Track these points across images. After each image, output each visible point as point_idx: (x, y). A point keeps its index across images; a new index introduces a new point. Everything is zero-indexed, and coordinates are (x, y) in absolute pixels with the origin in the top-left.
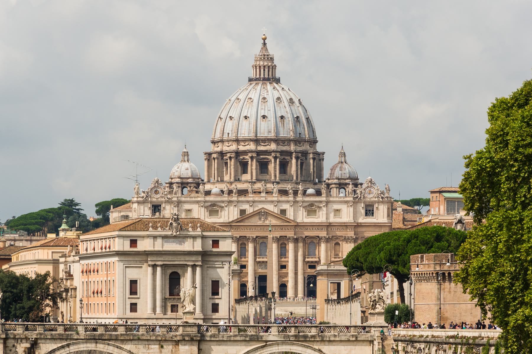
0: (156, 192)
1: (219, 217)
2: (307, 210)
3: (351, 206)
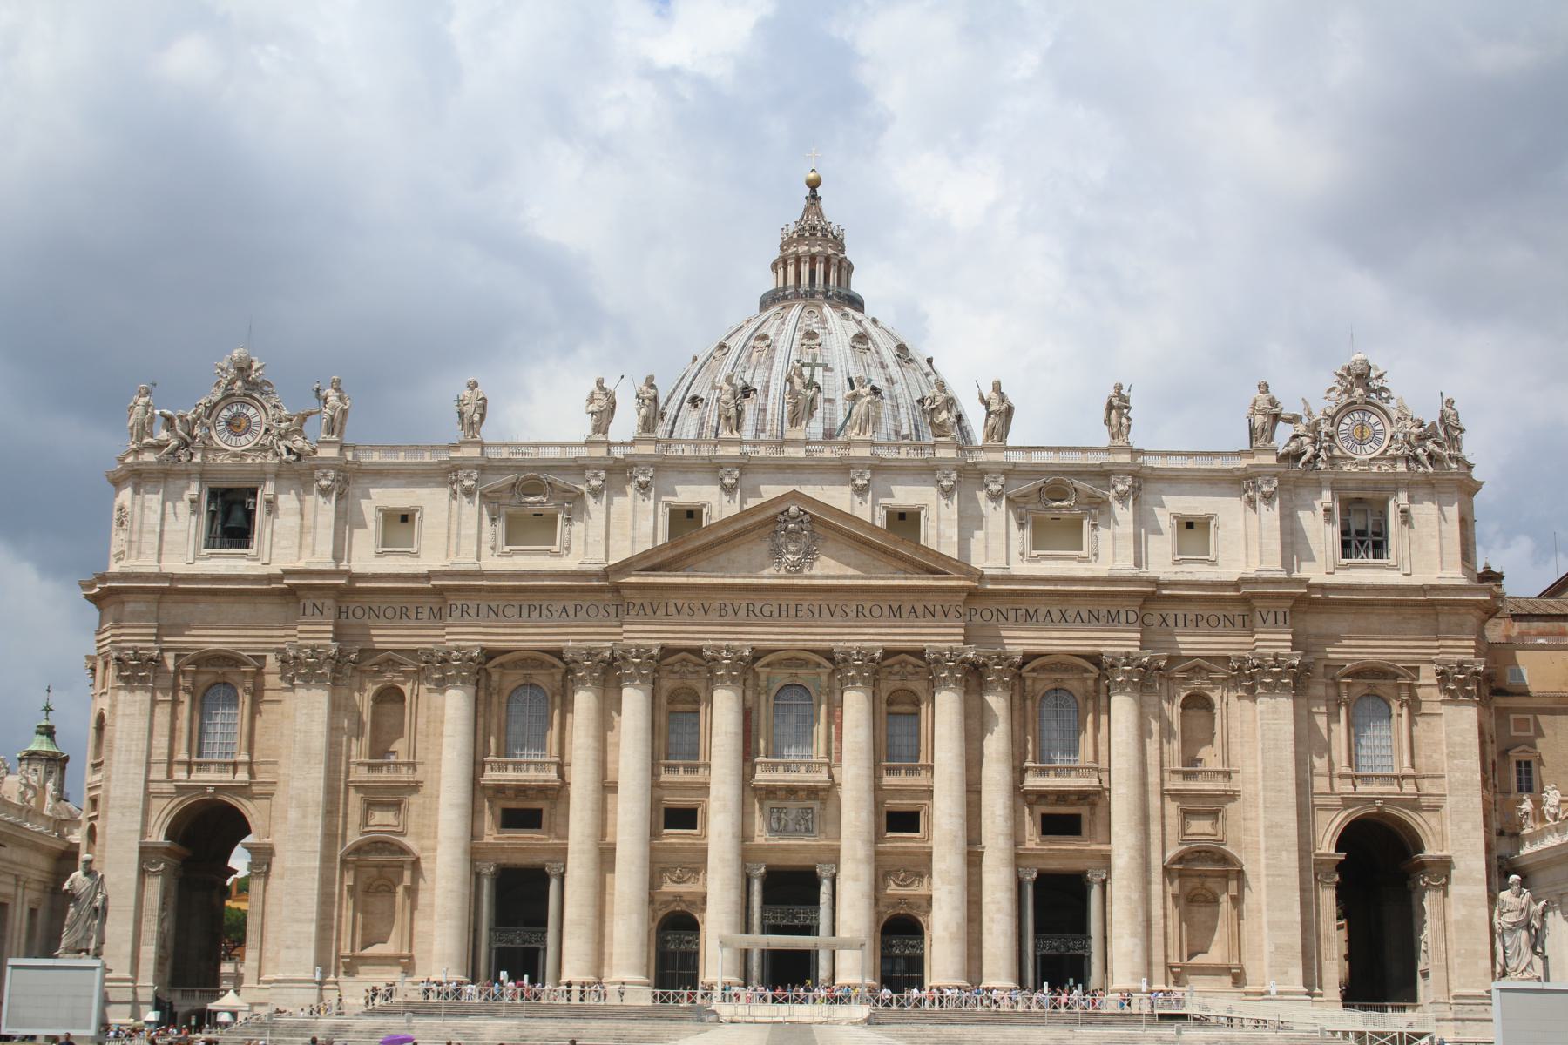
0: (236, 426)
1: (556, 548)
2: (1030, 517)
3: (1268, 498)
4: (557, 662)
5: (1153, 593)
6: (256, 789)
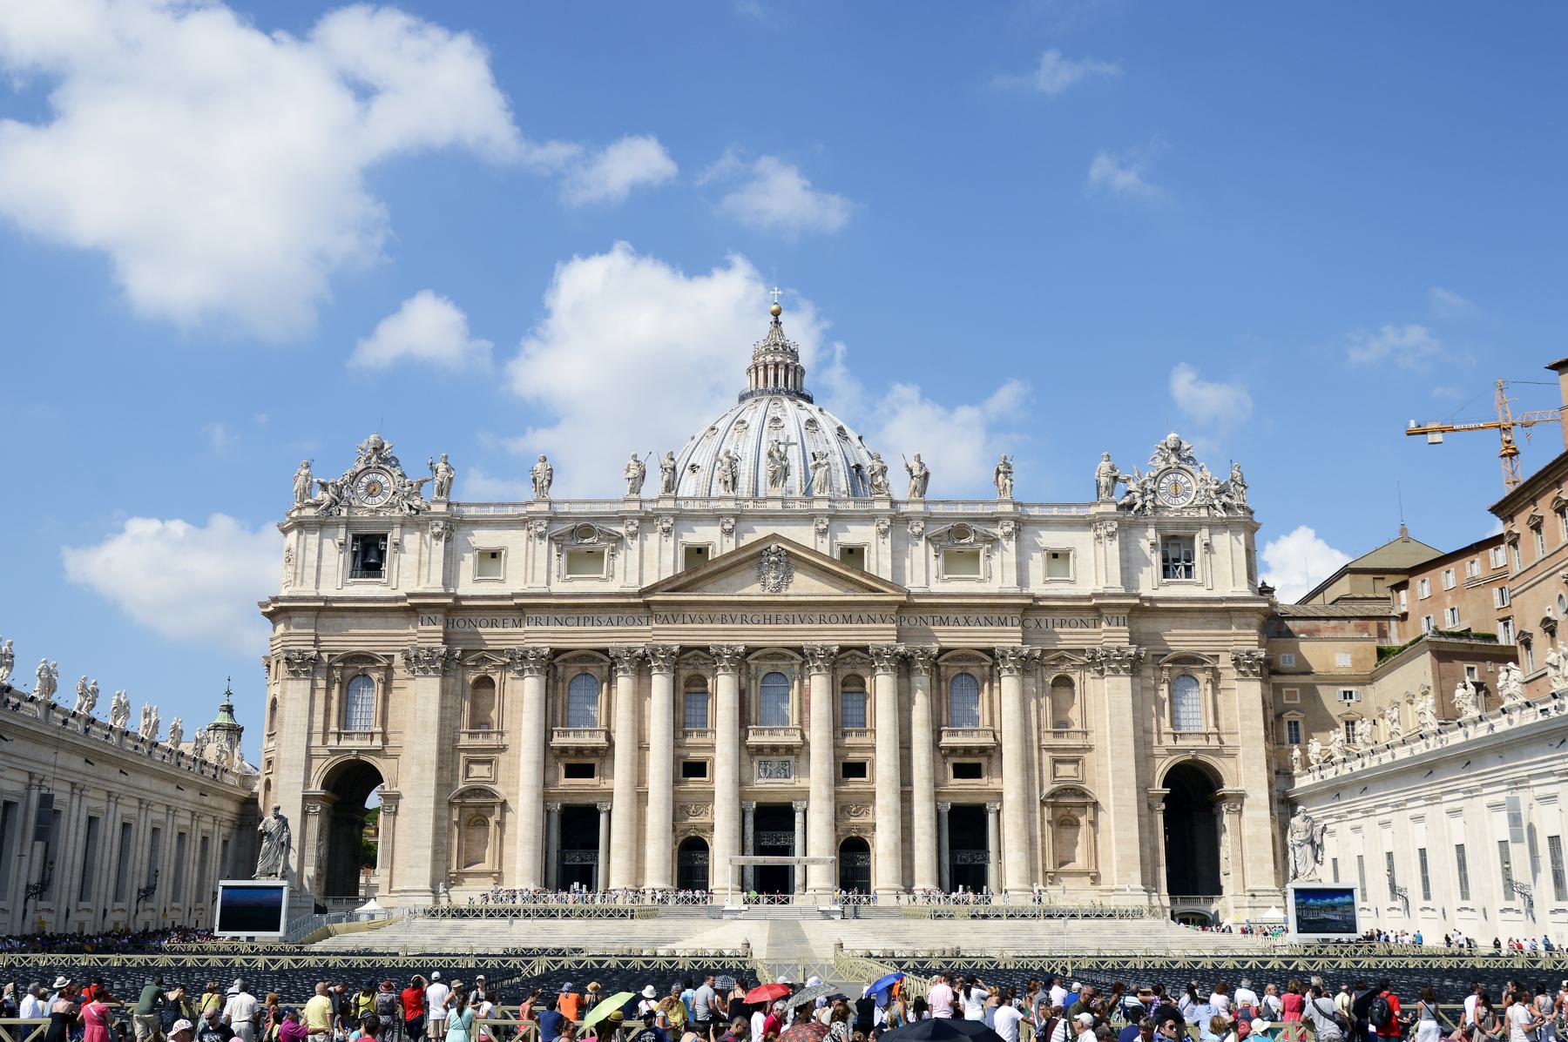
0: (373, 489)
1: (604, 576)
2: (942, 550)
3: (1111, 535)
4: (604, 657)
5: (1031, 604)
6: (389, 752)
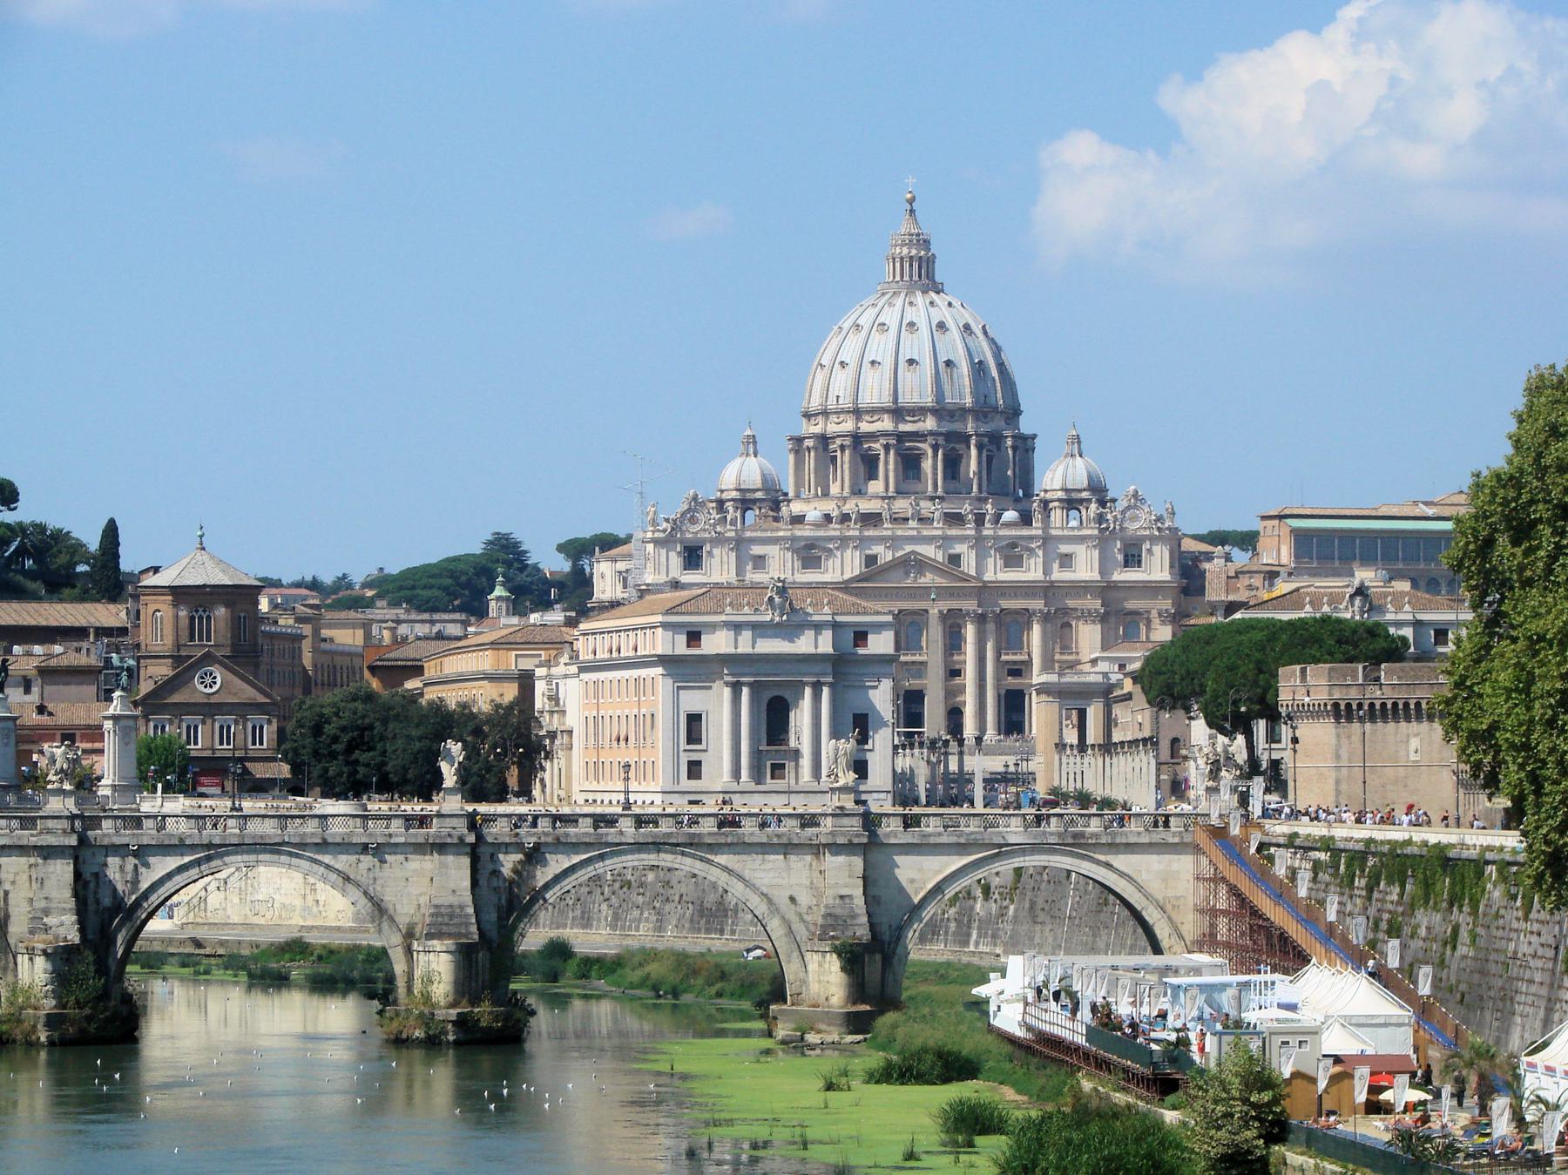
0: (693, 521)
